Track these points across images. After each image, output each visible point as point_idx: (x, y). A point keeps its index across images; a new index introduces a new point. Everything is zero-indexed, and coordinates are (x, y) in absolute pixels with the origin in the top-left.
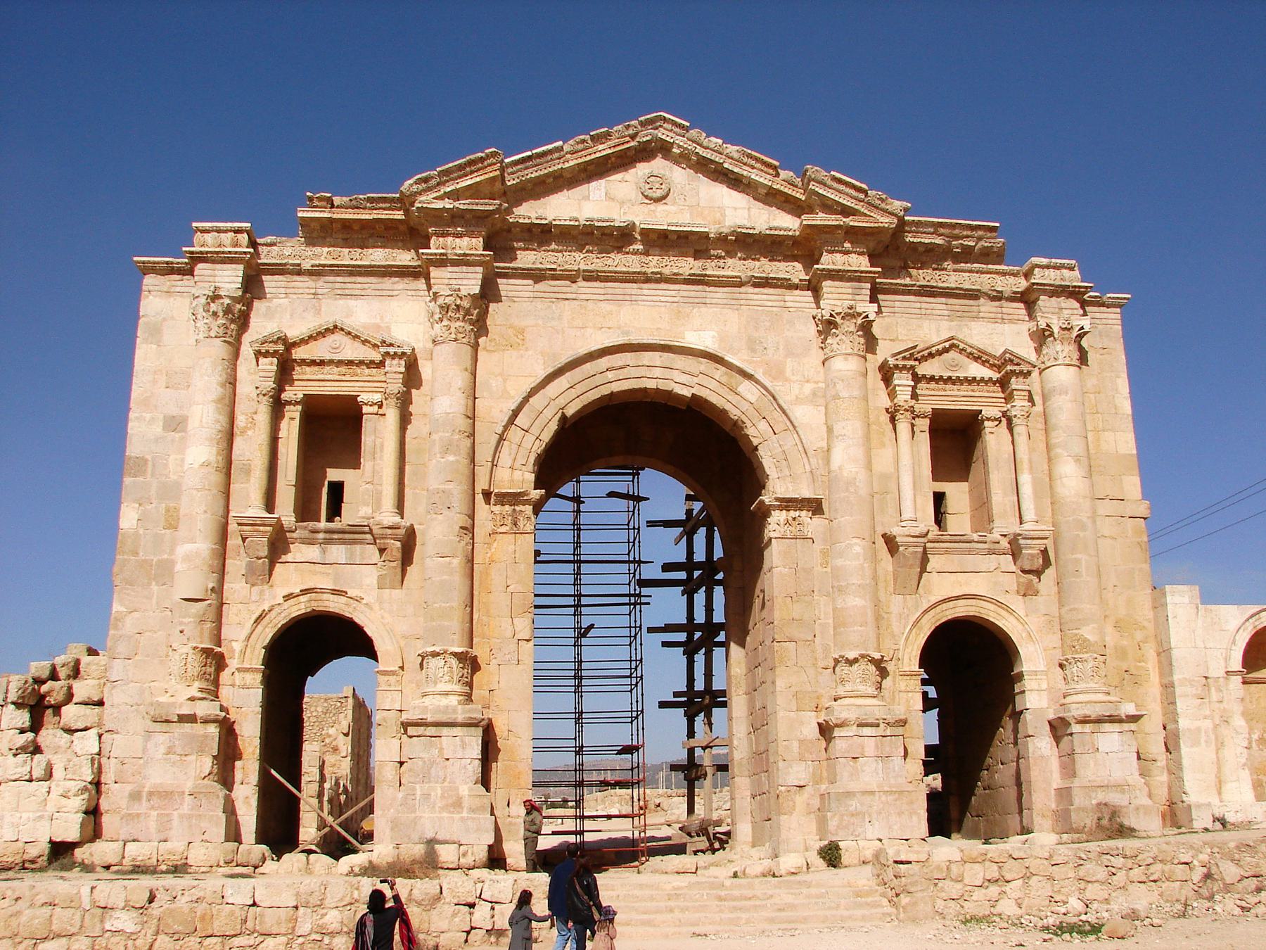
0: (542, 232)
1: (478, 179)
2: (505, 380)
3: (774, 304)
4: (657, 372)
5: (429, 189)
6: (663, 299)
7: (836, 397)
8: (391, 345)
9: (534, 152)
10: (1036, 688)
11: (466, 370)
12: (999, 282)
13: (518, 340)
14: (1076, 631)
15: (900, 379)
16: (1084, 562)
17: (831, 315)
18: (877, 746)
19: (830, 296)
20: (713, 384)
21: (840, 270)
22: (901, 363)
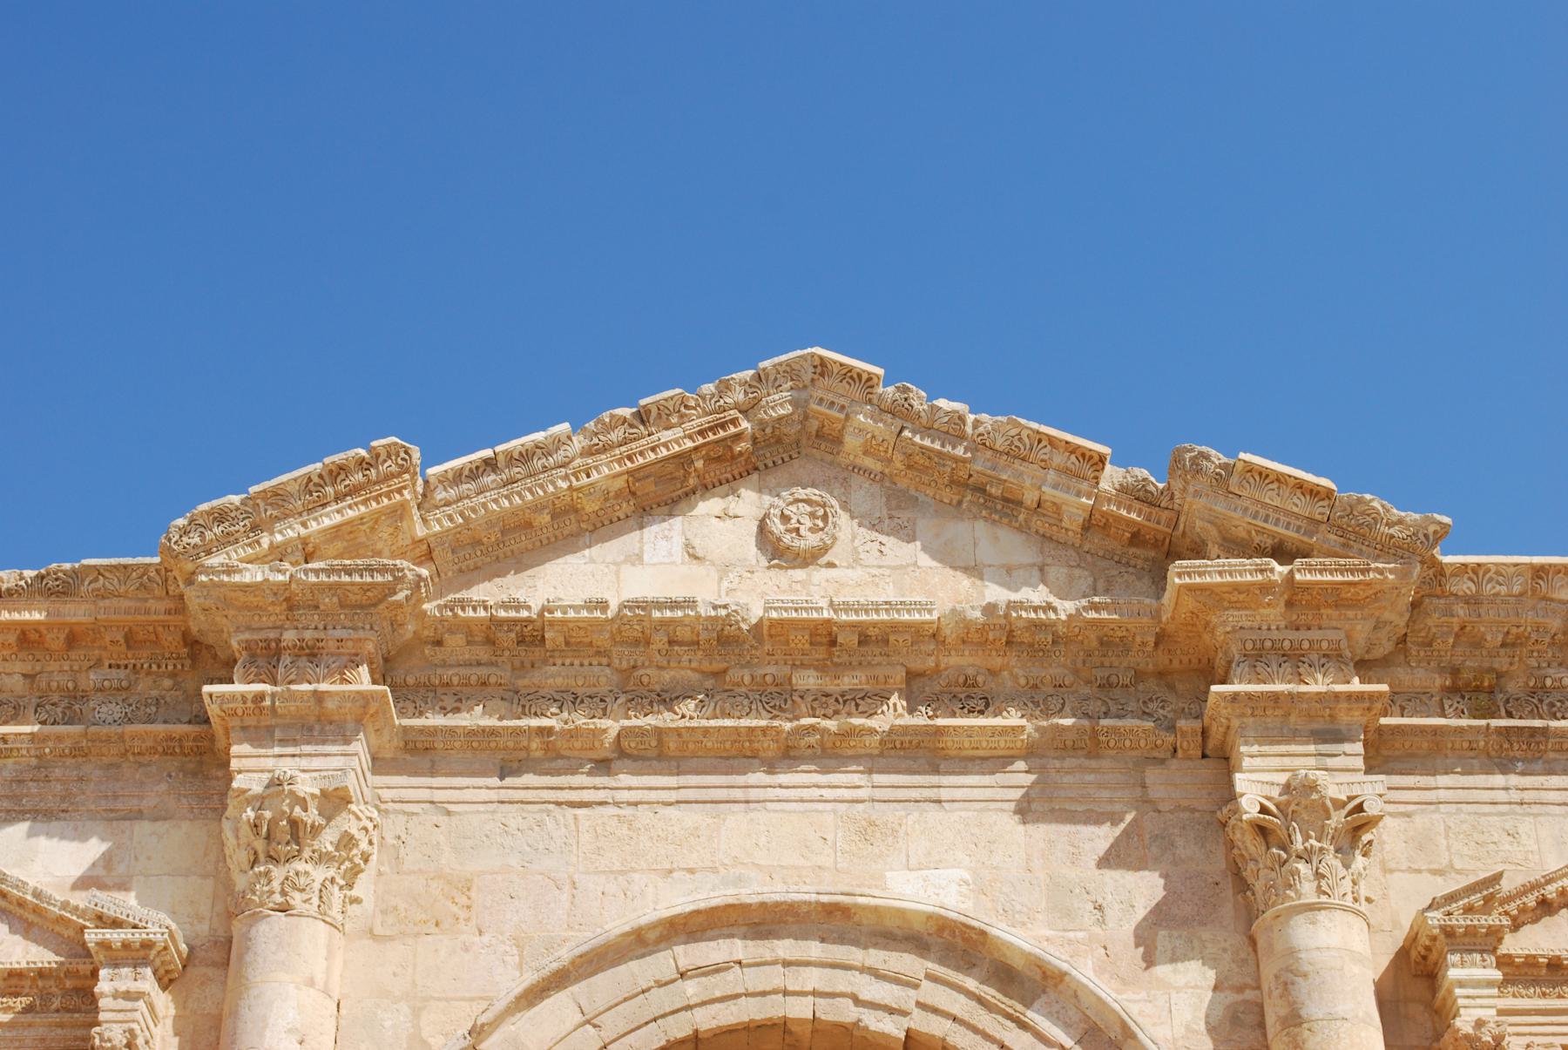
0: (521, 641)
1: (351, 514)
2: (416, 1013)
3: (1119, 794)
4: (813, 978)
5: (228, 540)
6: (828, 793)
8: (116, 924)
9: (499, 448)
11: (311, 983)
13: (455, 909)
15: (1463, 964)
17: (1264, 810)
19: (1258, 762)
20: (958, 1005)
21: (1275, 697)
22: (1459, 921)
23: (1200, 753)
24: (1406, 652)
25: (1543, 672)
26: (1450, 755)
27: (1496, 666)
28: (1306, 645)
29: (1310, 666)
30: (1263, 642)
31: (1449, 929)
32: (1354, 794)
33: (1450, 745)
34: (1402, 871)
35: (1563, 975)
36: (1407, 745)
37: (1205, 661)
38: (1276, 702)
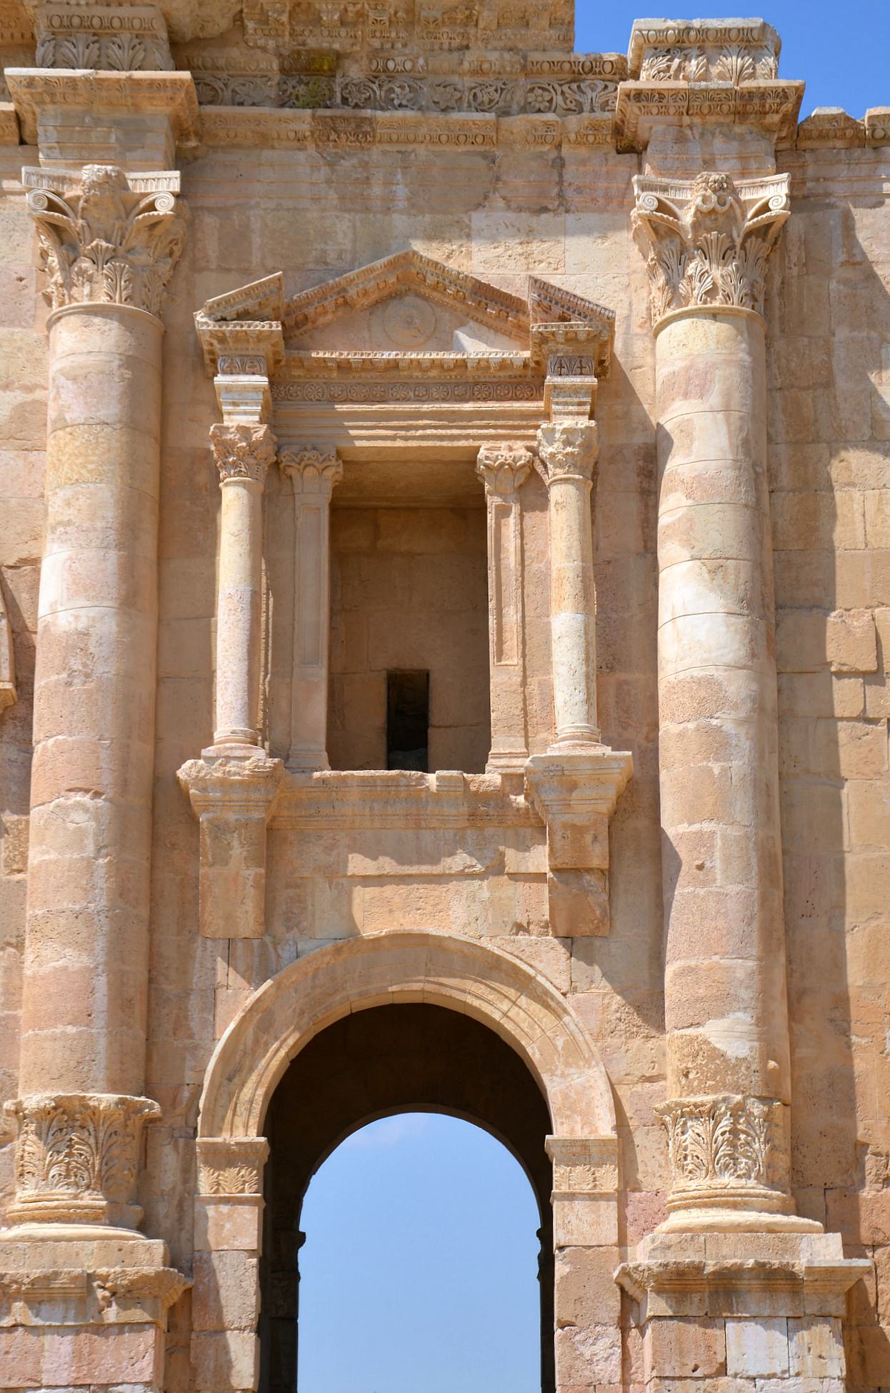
7: (61, 424)
10: (587, 1188)
12: (559, 99)
14: (691, 1032)
16: (719, 842)
17: (52, 206)
18: (77, 1355)
23: (17, 140)
24: (243, 28)
25: (386, 54)
26: (276, 145)
27: (336, 46)
28: (116, 23)
29: (119, 47)
30: (70, 18)
31: (220, 335)
32: (149, 191)
33: (275, 135)
34: (212, 270)
35: (354, 377)
36: (232, 134)
37: (28, 35)
38: (75, 89)
